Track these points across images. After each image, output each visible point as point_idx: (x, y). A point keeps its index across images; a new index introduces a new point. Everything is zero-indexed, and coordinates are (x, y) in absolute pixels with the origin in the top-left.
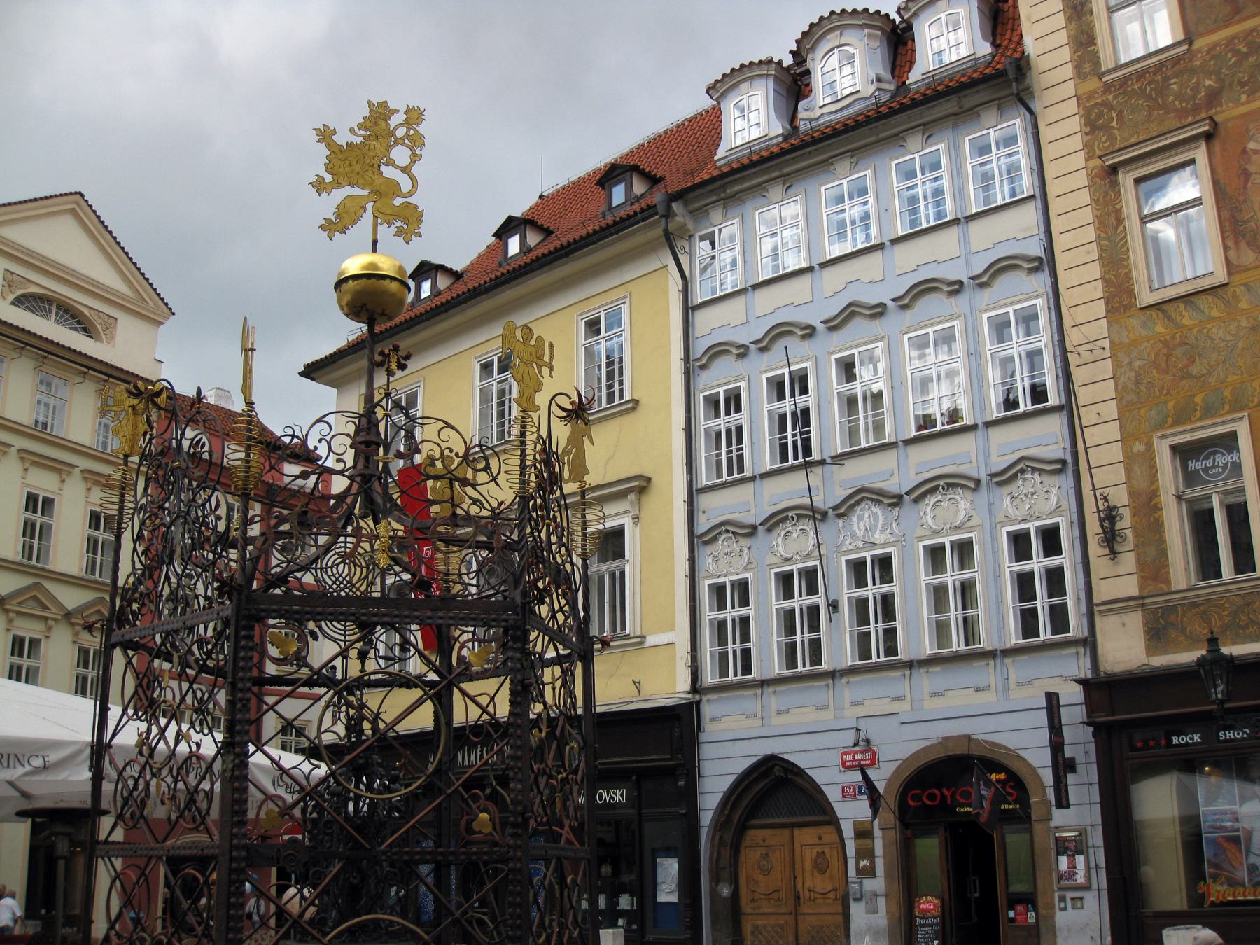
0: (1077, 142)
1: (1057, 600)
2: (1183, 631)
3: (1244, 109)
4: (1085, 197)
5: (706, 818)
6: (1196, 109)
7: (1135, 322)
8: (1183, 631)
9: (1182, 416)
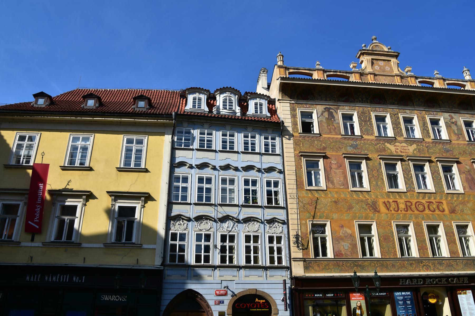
1: (279, 256)
2: (313, 268)
3: (331, 154)
4: (293, 159)
5: (163, 308)
8: (313, 268)
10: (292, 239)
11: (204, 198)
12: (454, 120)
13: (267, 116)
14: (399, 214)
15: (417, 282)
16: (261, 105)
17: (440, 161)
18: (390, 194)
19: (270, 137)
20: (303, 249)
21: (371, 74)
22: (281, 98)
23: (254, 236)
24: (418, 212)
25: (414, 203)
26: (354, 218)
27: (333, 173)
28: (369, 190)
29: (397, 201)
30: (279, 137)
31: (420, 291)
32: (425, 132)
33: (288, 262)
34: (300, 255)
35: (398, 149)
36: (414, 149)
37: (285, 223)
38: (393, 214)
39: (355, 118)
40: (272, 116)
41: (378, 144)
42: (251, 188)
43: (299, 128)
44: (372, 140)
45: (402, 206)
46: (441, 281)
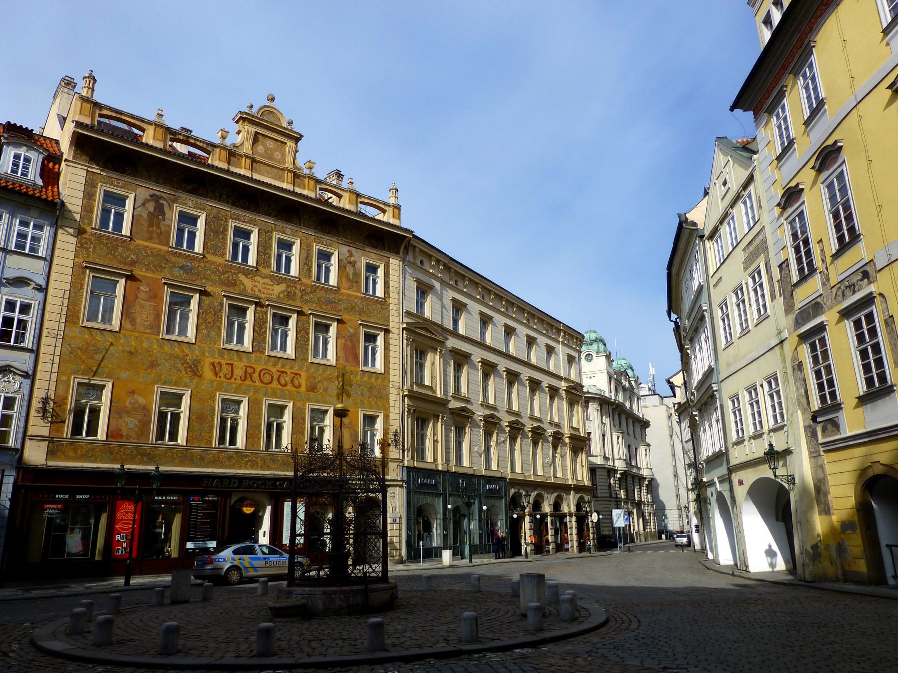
2: (64, 454)
6: (125, 264)
7: (77, 330)
8: (64, 454)
10: (36, 404)
12: (352, 259)
13: (35, 184)
15: (230, 484)
16: (27, 160)
17: (315, 315)
18: (226, 352)
19: (32, 224)
20: (52, 423)
21: (247, 157)
22: (71, 158)
24: (261, 385)
25: (258, 371)
26: (158, 381)
27: (137, 307)
28: (193, 341)
29: (232, 365)
30: (52, 226)
31: (231, 497)
32: (306, 268)
33: (20, 441)
34: (45, 431)
35: (256, 286)
37: (31, 377)
38: (222, 383)
39: (201, 224)
40: (46, 186)
41: (226, 272)
43: (94, 219)
44: (219, 265)
45: (239, 372)
46: (265, 484)
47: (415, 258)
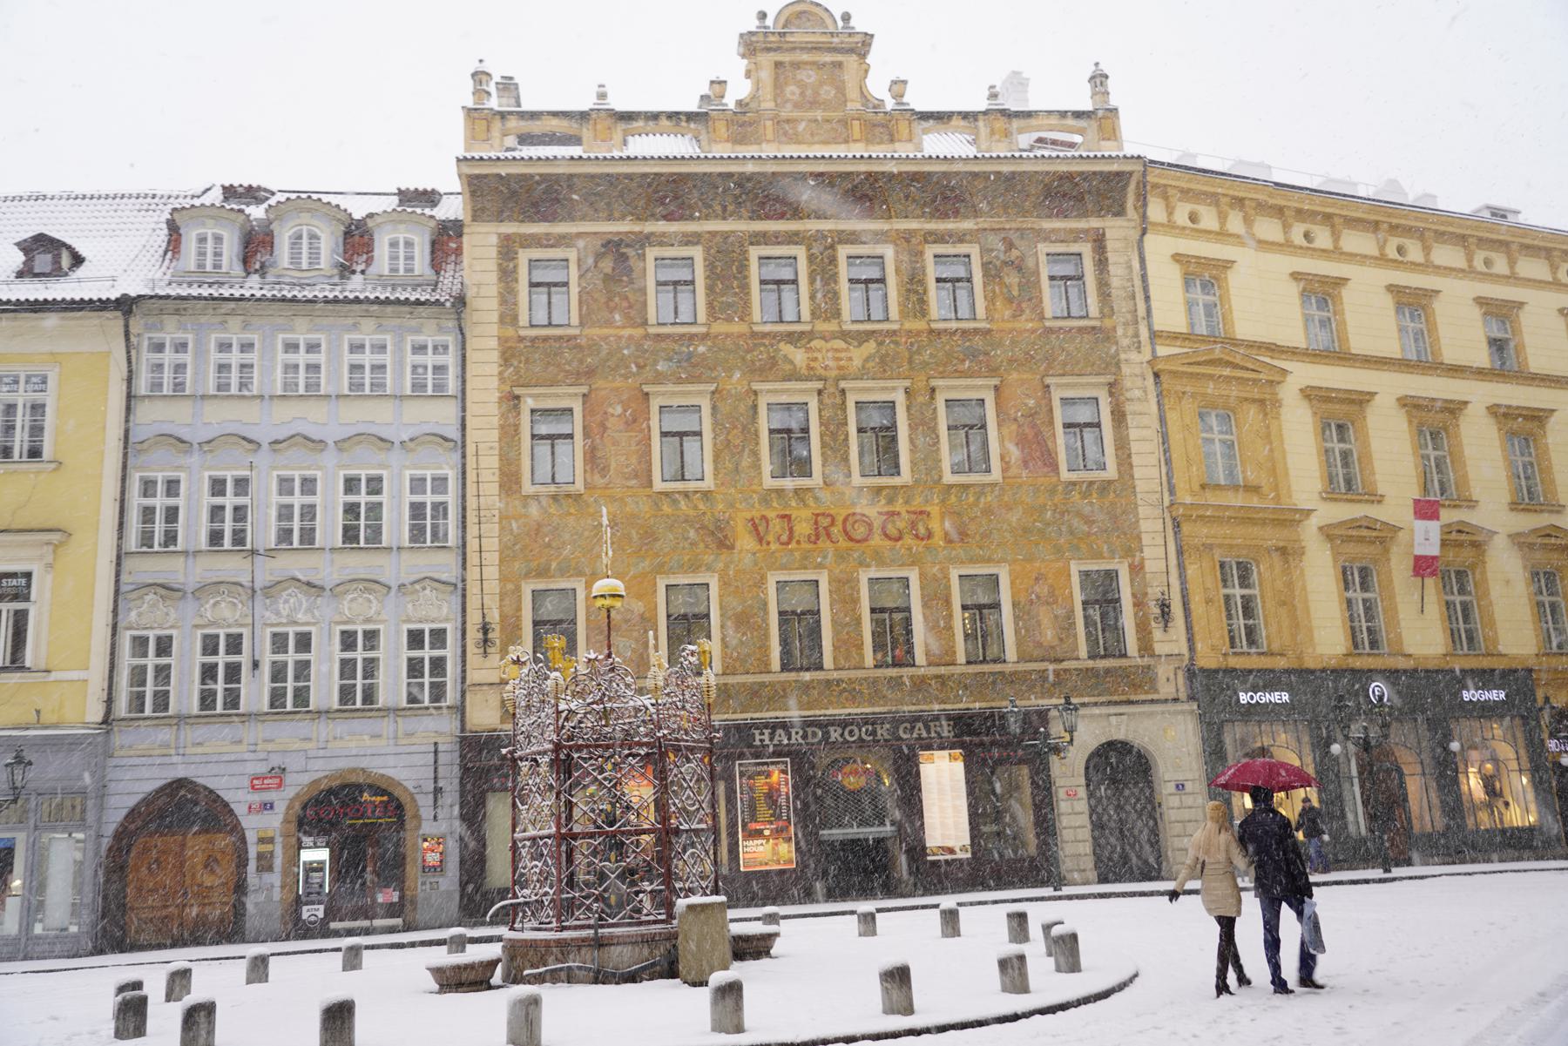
0: (495, 369)
4: (494, 409)
9: (543, 573)
10: (473, 635)
11: (226, 533)
14: (791, 551)
23: (366, 633)
24: (851, 544)
26: (660, 569)
35: (816, 359)
36: (866, 354)
42: (363, 498)
44: (741, 336)
45: (803, 528)
47: (1170, 211)
